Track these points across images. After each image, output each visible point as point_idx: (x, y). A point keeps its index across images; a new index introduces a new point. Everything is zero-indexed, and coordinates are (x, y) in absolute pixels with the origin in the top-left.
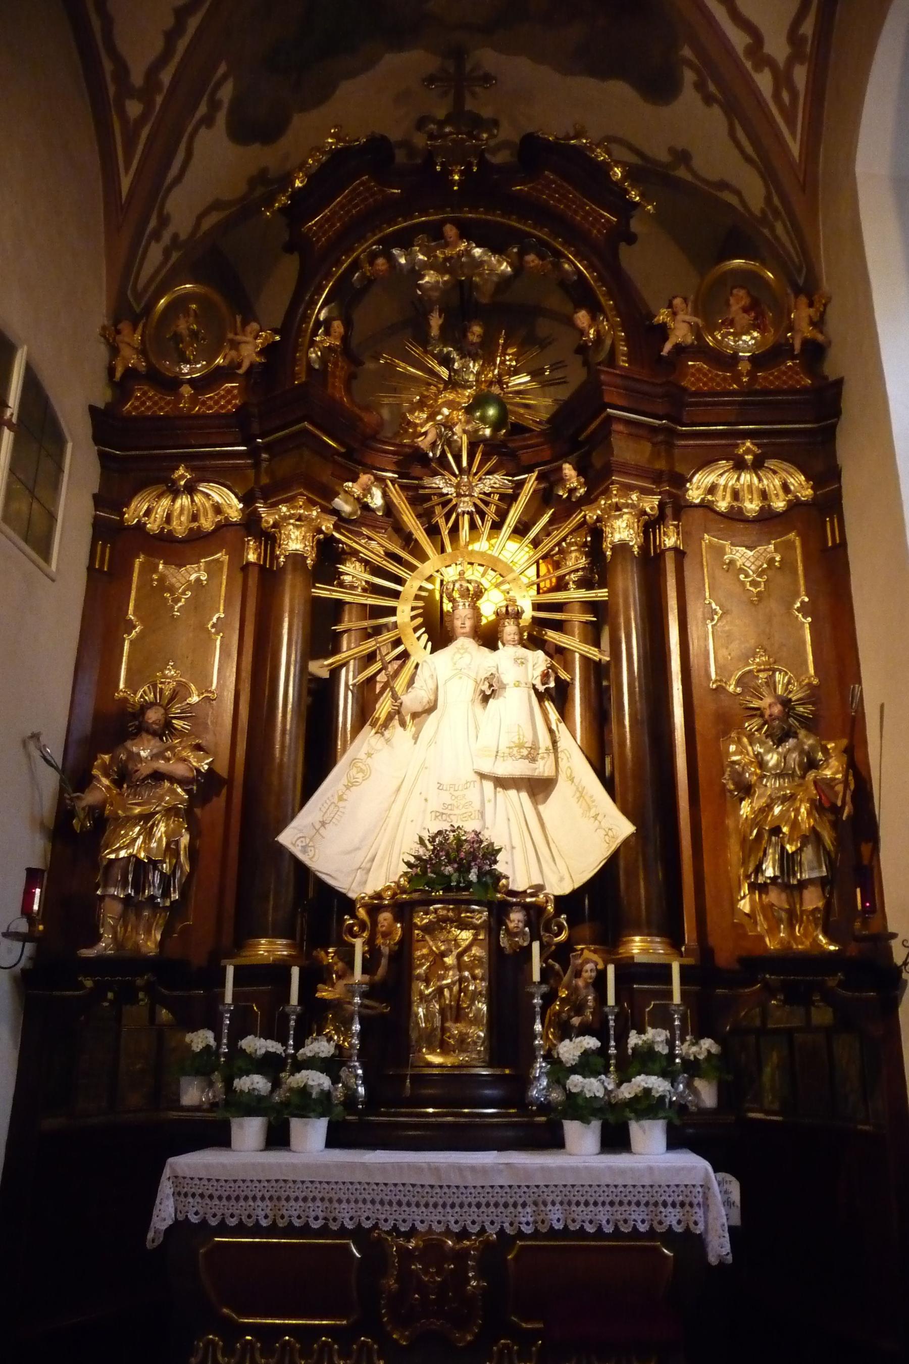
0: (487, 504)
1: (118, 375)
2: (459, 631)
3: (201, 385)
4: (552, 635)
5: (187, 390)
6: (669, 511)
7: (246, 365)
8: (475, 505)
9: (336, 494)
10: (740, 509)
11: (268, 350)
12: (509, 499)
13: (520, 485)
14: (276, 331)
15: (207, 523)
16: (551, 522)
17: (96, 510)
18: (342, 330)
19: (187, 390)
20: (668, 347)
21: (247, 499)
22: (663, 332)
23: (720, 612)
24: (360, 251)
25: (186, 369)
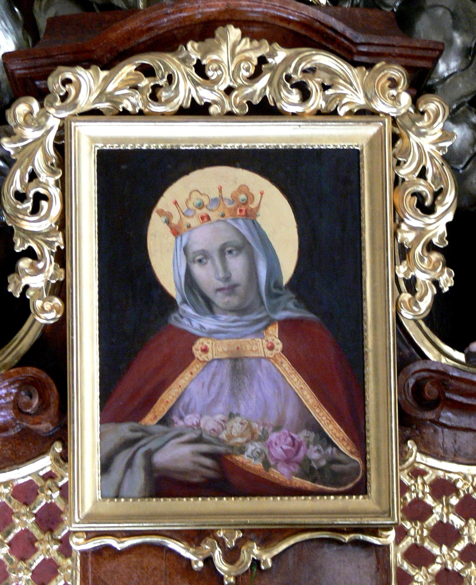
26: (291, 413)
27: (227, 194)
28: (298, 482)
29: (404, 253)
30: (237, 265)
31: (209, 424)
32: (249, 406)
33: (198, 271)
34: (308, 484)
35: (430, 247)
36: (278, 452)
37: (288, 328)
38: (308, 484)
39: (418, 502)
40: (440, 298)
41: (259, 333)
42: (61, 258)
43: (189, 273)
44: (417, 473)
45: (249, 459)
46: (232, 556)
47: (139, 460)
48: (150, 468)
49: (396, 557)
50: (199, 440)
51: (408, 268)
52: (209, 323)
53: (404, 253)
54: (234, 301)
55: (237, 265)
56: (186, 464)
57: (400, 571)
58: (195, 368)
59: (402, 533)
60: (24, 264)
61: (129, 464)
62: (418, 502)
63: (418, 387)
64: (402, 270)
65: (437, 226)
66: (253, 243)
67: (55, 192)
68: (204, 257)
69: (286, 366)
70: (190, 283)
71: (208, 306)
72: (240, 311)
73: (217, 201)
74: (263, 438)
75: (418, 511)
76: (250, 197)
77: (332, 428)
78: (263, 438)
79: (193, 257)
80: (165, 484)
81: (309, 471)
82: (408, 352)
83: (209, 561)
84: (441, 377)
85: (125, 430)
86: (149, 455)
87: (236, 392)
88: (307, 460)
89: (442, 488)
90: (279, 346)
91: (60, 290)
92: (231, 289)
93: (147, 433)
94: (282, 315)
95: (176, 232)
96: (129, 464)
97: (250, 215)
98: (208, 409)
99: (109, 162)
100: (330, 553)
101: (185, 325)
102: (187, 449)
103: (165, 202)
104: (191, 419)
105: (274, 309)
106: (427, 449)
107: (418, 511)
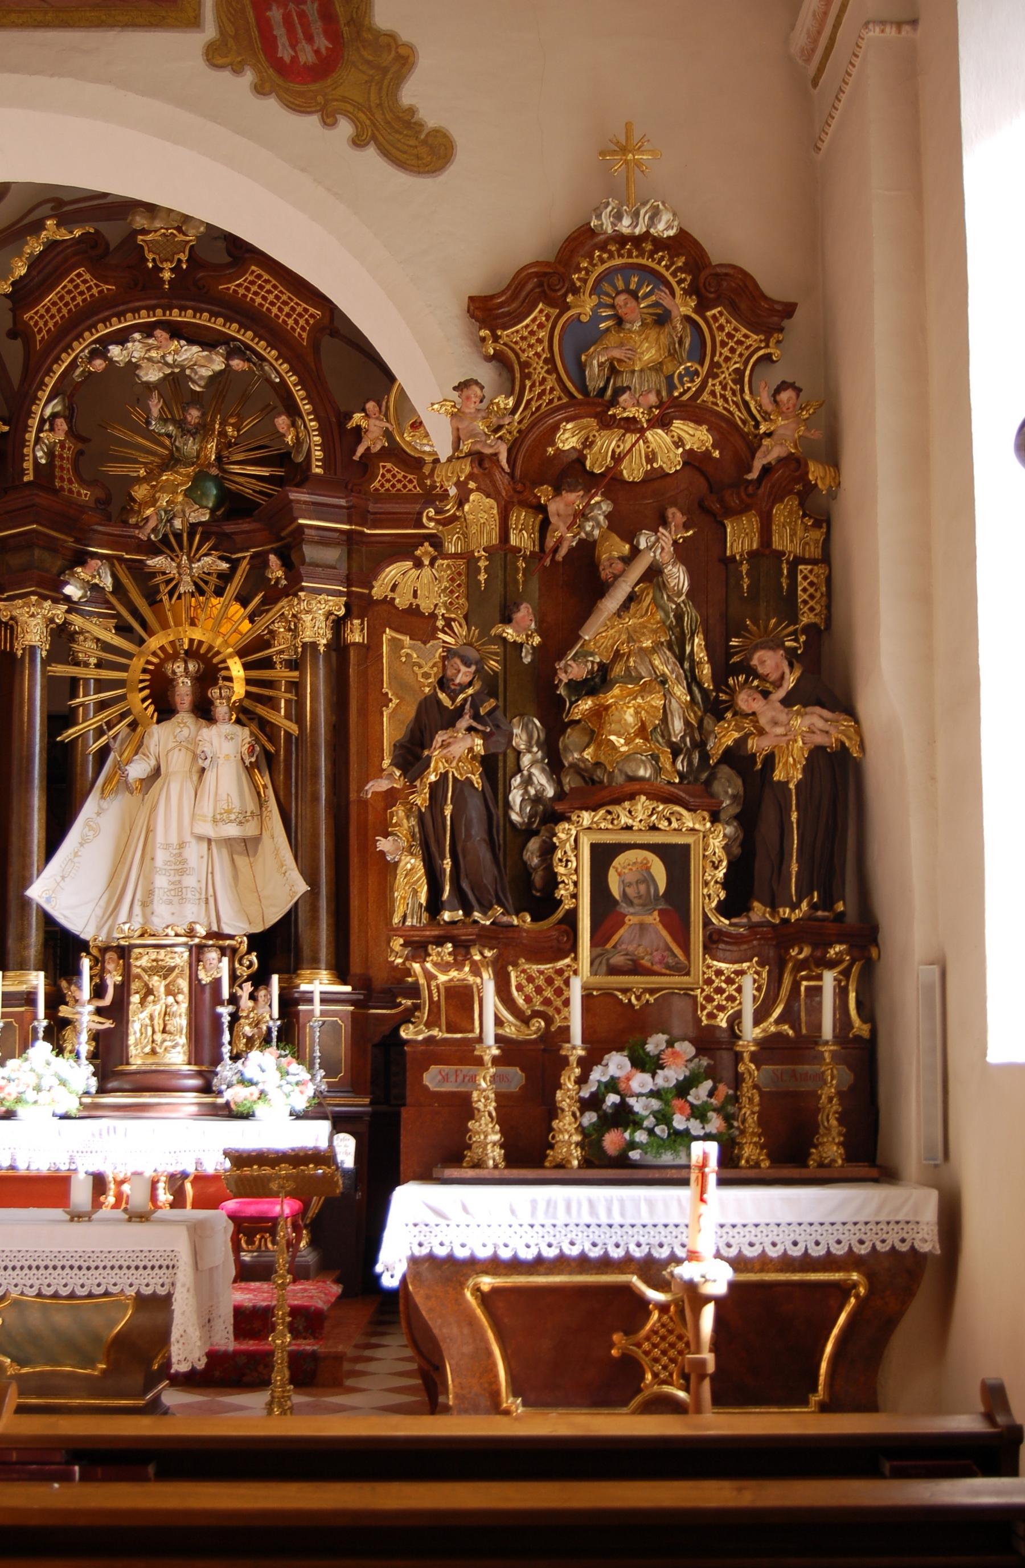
0: (206, 583)
4: (261, 710)
6: (355, 610)
8: (196, 584)
9: (67, 583)
10: (418, 606)
12: (225, 578)
13: (235, 564)
16: (263, 603)
18: (65, 427)
20: (361, 450)
22: (358, 433)
23: (395, 701)
24: (81, 348)
26: (662, 945)
27: (639, 860)
28: (664, 971)
29: (706, 884)
30: (642, 888)
31: (631, 948)
32: (645, 942)
33: (627, 890)
34: (668, 972)
35: (716, 882)
36: (657, 959)
37: (661, 913)
38: (668, 972)
39: (709, 979)
40: (719, 901)
41: (651, 914)
42: (576, 884)
43: (624, 891)
44: (709, 967)
45: (645, 962)
46: (638, 998)
47: (604, 961)
48: (608, 965)
49: (700, 999)
50: (627, 954)
51: (707, 890)
52: (631, 910)
53: (706, 884)
54: (641, 901)
55: (642, 888)
56: (621, 964)
57: (702, 1005)
58: (626, 927)
59: (703, 990)
60: (561, 886)
61: (600, 963)
62: (709, 979)
63: (710, 936)
64: (705, 891)
65: (720, 874)
66: (649, 879)
67: (573, 859)
68: (630, 885)
69: (660, 927)
70: (624, 895)
71: (631, 903)
72: (644, 905)
73: (635, 863)
74: (651, 954)
75: (709, 982)
76: (648, 862)
77: (677, 951)
78: (651, 954)
79: (624, 884)
80: (613, 971)
81: (668, 967)
82: (707, 922)
83: (630, 1000)
84: (720, 932)
85: (599, 950)
86: (608, 960)
87: (641, 936)
88: (667, 963)
89: (719, 973)
90: (658, 919)
91: (575, 896)
92: (640, 897)
93: (607, 951)
94: (660, 907)
95: (619, 874)
96: (600, 963)
97: (648, 869)
98: (630, 943)
99: (594, 847)
100: (676, 998)
101: (622, 910)
102: (622, 958)
103: (615, 863)
104: (624, 946)
105: (656, 905)
106: (713, 958)
107: (709, 982)
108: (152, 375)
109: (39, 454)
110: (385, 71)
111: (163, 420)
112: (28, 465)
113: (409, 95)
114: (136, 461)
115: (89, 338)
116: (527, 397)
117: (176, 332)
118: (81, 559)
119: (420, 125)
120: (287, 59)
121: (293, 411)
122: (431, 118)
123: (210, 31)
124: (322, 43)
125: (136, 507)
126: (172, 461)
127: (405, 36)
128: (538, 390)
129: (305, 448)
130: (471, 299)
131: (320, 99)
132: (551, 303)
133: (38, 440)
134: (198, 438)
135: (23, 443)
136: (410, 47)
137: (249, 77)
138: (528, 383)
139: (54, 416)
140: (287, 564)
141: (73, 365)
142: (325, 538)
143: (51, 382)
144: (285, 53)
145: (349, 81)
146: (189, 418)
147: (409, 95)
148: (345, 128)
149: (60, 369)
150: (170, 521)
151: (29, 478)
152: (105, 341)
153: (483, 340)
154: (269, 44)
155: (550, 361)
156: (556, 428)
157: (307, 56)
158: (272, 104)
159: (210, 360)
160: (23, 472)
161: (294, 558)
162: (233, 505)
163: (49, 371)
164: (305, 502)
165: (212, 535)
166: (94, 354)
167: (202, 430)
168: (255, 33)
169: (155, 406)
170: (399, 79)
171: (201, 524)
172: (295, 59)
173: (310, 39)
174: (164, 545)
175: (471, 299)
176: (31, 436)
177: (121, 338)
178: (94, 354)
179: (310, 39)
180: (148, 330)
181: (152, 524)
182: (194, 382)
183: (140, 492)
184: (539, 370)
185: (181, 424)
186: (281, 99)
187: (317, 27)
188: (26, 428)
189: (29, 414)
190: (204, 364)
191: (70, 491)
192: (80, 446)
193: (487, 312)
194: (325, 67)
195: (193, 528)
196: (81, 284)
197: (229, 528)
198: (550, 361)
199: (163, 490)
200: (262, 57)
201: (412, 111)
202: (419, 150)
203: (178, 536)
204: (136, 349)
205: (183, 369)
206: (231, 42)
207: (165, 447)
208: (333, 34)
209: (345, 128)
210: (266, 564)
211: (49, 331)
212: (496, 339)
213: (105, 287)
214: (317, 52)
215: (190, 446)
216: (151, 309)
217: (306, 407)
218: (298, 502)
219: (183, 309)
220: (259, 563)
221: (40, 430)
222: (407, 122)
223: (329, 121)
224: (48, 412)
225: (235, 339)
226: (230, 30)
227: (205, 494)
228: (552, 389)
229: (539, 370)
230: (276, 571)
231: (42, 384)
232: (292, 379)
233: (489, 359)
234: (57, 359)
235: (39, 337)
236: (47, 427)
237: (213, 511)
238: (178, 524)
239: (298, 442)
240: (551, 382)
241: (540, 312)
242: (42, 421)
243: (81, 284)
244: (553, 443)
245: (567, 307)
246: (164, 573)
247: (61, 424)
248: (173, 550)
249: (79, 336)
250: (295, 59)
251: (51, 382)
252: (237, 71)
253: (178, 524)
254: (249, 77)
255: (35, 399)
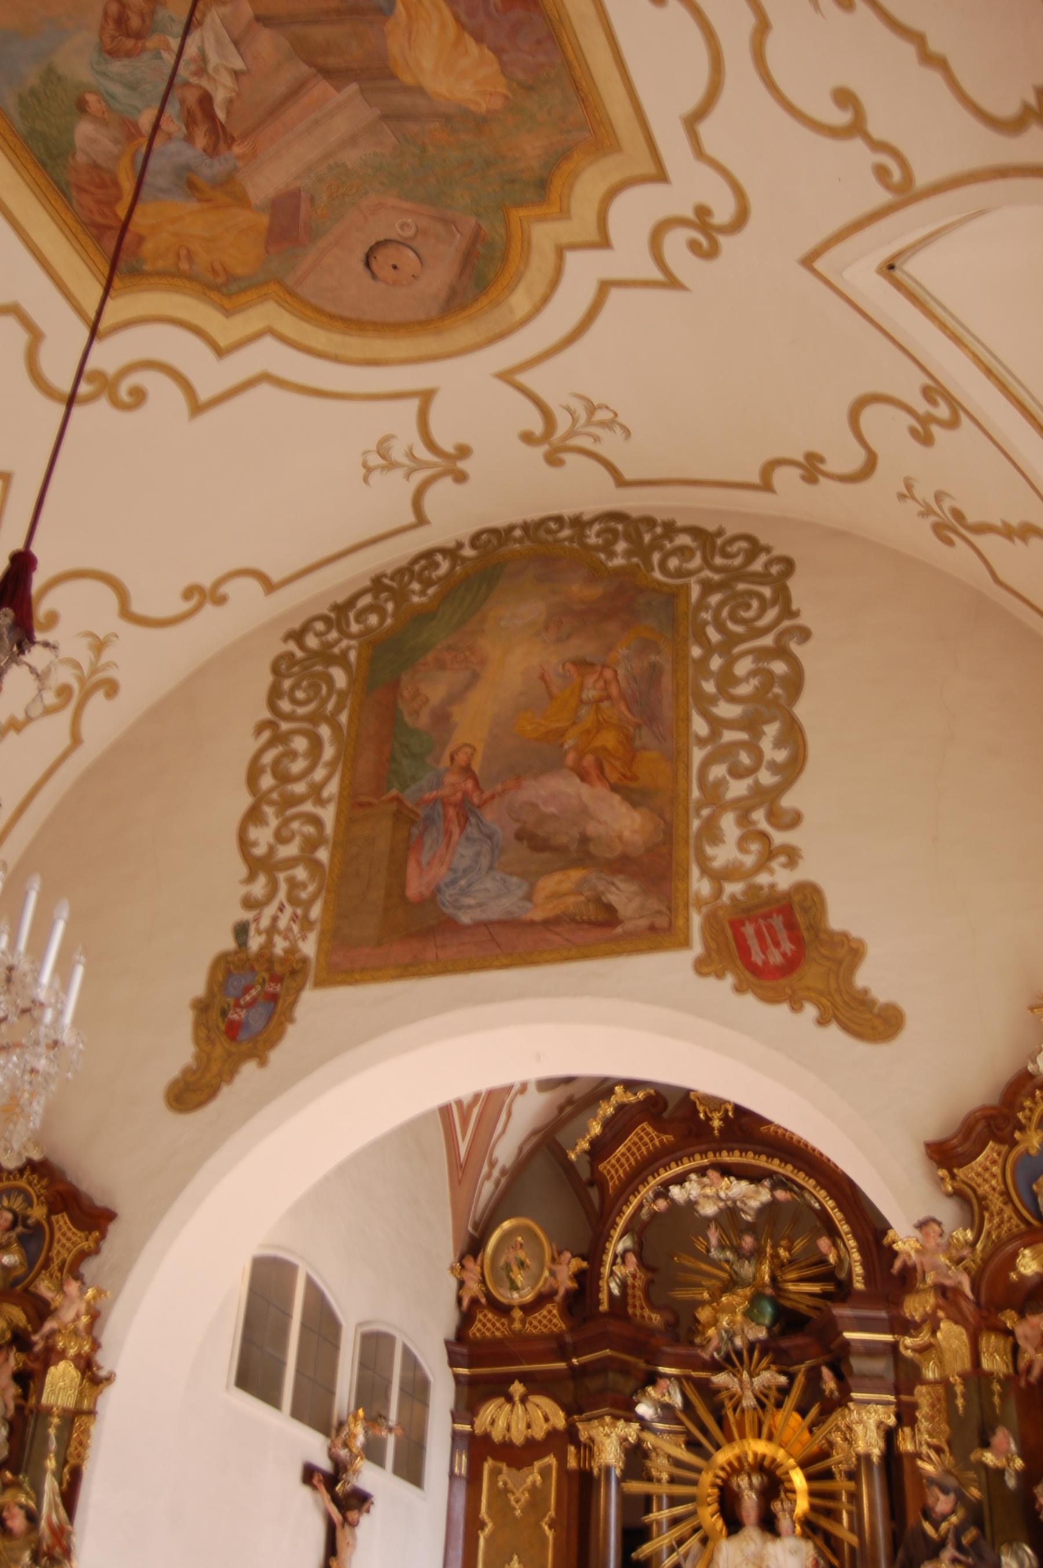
0: (766, 1396)
1: (466, 1302)
2: (746, 1520)
3: (528, 1309)
5: (517, 1314)
7: (562, 1292)
11: (579, 1276)
12: (784, 1391)
13: (792, 1377)
14: (584, 1258)
15: (539, 1432)
17: (454, 1421)
19: (517, 1314)
21: (569, 1413)
24: (646, 1191)
25: (516, 1295)
108: (709, 1209)
109: (613, 1285)
110: (840, 962)
111: (722, 1247)
112: (604, 1296)
113: (864, 978)
114: (699, 1285)
115: (653, 1182)
116: (987, 1226)
117: (726, 1171)
118: (652, 1379)
119: (874, 1002)
120: (760, 963)
121: (833, 1233)
122: (881, 995)
123: (697, 948)
124: (788, 947)
125: (700, 1328)
126: (731, 1284)
127: (855, 933)
128: (996, 1220)
129: (846, 1265)
130: (928, 1146)
131: (789, 991)
132: (1000, 1141)
133: (612, 1273)
134: (753, 1261)
135: (599, 1276)
136: (861, 942)
137: (730, 979)
138: (987, 1215)
139: (626, 1251)
140: (840, 1376)
141: (641, 1206)
142: (871, 1351)
143: (622, 1222)
144: (757, 958)
145: (811, 974)
146: (744, 1244)
147: (864, 978)
148: (810, 1011)
149: (629, 1211)
150: (731, 1339)
151: (604, 1307)
152: (666, 1185)
153: (942, 1179)
154: (744, 951)
155: (1006, 1193)
156: (1015, 1255)
157: (776, 958)
158: (749, 1000)
159: (758, 1192)
160: (598, 1302)
161: (844, 1369)
162: (789, 1321)
163: (621, 1212)
164: (849, 1318)
165: (771, 1351)
166: (658, 1195)
167: (757, 1254)
168: (733, 945)
169: (713, 1235)
170: (853, 967)
171: (759, 1341)
172: (766, 962)
173: (777, 944)
174: (728, 1362)
175: (928, 1146)
176: (606, 1271)
177: (680, 1180)
178: (658, 1195)
179: (777, 944)
180: (702, 1172)
181: (714, 1343)
182: (745, 1212)
183: (704, 1314)
184: (996, 1202)
185: (737, 1250)
186: (755, 994)
187: (783, 935)
188: (601, 1263)
189: (604, 1251)
190: (752, 1197)
191: (643, 1317)
192: (650, 1275)
193: (945, 1155)
194: (791, 965)
195: (751, 1346)
196: (645, 1137)
197: (785, 1343)
198: (1006, 1193)
199: (723, 1310)
200: (739, 963)
201: (866, 991)
202: (874, 1022)
203: (739, 1353)
204: (692, 1189)
205: (734, 1202)
206: (714, 955)
207: (725, 1271)
208: (796, 939)
209: (810, 1011)
210: (819, 1377)
211: (619, 1178)
212: (953, 1177)
213: (664, 1138)
214: (784, 955)
215: (747, 1269)
216: (704, 1153)
217: (844, 1228)
218: (842, 1317)
219: (730, 1150)
220: (814, 1377)
221: (614, 1263)
222: (863, 1001)
223: (796, 1007)
224: (620, 1248)
225: (776, 1173)
226: (713, 945)
227: (761, 1313)
228: (1010, 1218)
229: (996, 1202)
230: (830, 1384)
231: (614, 1225)
232: (829, 1204)
233: (949, 1195)
234: (627, 1202)
235: (611, 1184)
236: (619, 1260)
237: (769, 1329)
238: (738, 1342)
239: (840, 1260)
240: (1008, 1212)
241: (991, 1150)
242: (615, 1256)
243: (645, 1137)
244: (1014, 1267)
245: (1014, 1143)
246: (727, 1389)
247: (632, 1259)
248: (734, 1366)
249: (644, 1181)
250: (766, 962)
251: (622, 1222)
252: (720, 976)
253: (738, 1342)
254: (730, 979)
255: (608, 1237)
